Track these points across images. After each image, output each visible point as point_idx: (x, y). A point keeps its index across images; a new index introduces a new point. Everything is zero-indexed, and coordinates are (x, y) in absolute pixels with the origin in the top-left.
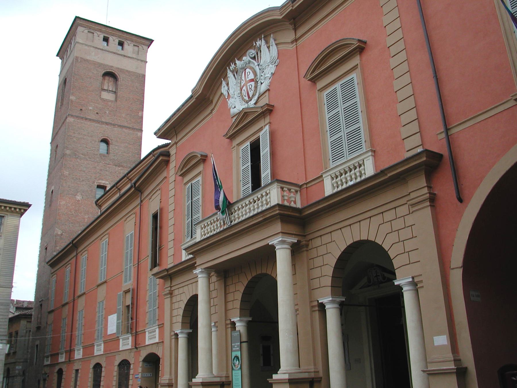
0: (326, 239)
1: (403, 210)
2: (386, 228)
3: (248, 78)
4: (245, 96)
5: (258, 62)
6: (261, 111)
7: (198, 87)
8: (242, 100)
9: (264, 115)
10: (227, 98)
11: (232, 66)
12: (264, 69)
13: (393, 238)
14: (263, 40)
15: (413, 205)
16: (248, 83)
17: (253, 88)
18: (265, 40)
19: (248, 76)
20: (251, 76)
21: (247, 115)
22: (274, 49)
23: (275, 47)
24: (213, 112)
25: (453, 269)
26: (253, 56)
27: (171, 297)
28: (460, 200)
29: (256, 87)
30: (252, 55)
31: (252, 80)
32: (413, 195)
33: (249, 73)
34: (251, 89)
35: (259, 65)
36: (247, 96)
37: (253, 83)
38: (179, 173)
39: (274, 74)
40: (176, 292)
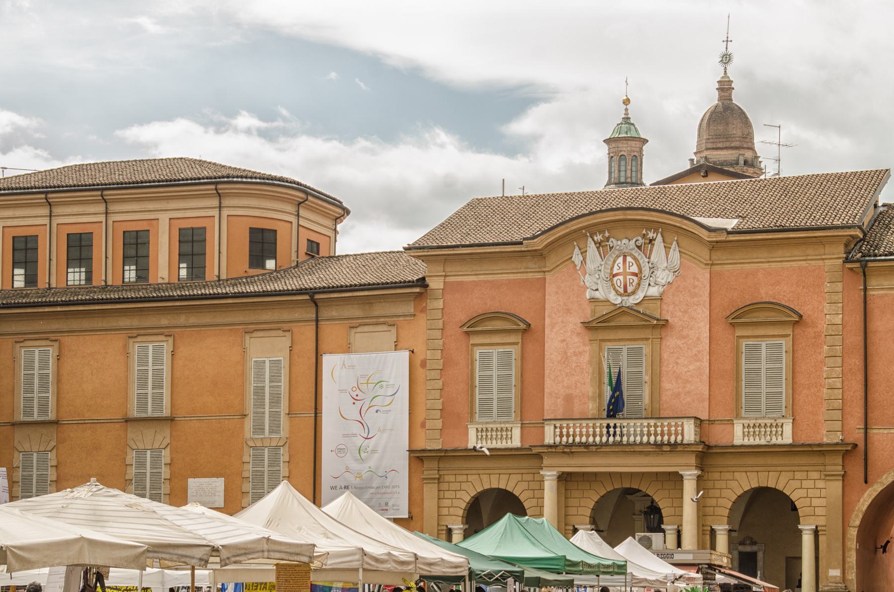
0: (728, 476)
1: (815, 475)
2: (797, 484)
4: (619, 287)
5: (649, 258)
10: (578, 268)
11: (598, 238)
13: (802, 493)
15: (826, 475)
16: (629, 275)
17: (634, 284)
18: (662, 236)
19: (629, 266)
20: (634, 269)
22: (675, 254)
23: (677, 254)
25: (851, 527)
27: (439, 483)
28: (866, 482)
29: (639, 284)
31: (635, 275)
32: (828, 468)
33: (631, 264)
35: (649, 263)
36: (623, 289)
37: (635, 278)
38: (465, 329)
40: (447, 478)
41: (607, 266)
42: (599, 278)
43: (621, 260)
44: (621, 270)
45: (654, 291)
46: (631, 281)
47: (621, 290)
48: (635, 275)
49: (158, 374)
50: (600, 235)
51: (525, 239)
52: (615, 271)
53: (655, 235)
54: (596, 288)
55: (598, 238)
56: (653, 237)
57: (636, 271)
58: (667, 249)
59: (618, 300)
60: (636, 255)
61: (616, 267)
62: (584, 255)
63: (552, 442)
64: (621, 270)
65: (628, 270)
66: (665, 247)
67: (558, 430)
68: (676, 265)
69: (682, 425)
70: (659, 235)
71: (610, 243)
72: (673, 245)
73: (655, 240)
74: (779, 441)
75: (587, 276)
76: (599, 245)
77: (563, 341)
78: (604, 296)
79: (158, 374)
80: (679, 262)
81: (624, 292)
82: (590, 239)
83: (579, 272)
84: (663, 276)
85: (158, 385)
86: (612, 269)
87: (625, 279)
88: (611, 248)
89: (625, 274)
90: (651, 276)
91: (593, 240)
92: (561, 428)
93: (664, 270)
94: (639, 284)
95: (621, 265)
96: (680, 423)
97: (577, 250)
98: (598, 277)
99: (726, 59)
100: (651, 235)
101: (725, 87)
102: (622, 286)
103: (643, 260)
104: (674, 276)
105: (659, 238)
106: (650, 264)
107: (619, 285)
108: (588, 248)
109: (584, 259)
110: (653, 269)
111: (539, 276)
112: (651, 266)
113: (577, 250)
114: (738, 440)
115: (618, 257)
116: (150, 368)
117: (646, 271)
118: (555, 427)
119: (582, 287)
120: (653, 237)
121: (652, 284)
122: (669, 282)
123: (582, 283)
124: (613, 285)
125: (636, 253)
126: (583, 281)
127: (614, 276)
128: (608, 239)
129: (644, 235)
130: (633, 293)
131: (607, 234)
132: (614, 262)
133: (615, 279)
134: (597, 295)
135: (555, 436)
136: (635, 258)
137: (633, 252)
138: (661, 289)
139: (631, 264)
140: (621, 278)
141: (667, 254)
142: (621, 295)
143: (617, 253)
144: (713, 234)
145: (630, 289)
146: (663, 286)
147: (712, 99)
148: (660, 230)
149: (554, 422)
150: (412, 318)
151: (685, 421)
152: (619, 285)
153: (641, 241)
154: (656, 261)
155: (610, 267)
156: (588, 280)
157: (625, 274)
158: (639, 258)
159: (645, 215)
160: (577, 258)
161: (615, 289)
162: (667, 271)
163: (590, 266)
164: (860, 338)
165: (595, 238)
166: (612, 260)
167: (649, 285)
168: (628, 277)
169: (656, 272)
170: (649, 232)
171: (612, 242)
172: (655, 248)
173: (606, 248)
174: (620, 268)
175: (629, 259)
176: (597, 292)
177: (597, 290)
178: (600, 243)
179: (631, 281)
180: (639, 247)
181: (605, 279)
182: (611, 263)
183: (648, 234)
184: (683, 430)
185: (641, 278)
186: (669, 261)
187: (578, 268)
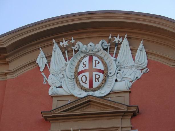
3: (95, 66)
4: (85, 83)
5: (116, 57)
6: (126, 110)
7: (6, 39)
8: (75, 82)
9: (123, 116)
10: (42, 70)
11: (65, 43)
12: (121, 68)
14: (125, 39)
16: (95, 72)
17: (101, 79)
19: (95, 64)
20: (101, 66)
21: (90, 104)
24: (8, 76)
26: (106, 47)
29: (105, 81)
30: (105, 46)
31: (102, 72)
33: (97, 62)
34: (98, 79)
35: (115, 61)
37: (102, 75)
39: (139, 79)
41: (72, 67)
42: (63, 77)
43: (87, 59)
44: (87, 67)
45: (123, 86)
46: (97, 77)
47: (87, 86)
48: (102, 72)
50: (66, 41)
52: (80, 69)
53: (121, 40)
54: (60, 85)
55: (65, 43)
56: (119, 41)
57: (103, 69)
58: (134, 52)
60: (102, 56)
61: (81, 65)
62: (49, 59)
64: (87, 67)
65: (94, 67)
66: (131, 49)
68: (143, 63)
70: (125, 39)
71: (76, 46)
72: (139, 49)
73: (121, 44)
75: (50, 76)
76: (64, 50)
78: (69, 92)
80: (146, 61)
81: (89, 87)
82: (56, 45)
83: (43, 74)
86: (77, 67)
88: (76, 52)
90: (117, 73)
93: (132, 68)
95: (87, 64)
97: (42, 54)
98: (62, 76)
100: (117, 39)
102: (88, 82)
103: (109, 59)
104: (142, 73)
105: (125, 42)
106: (117, 62)
107: (84, 81)
108: (53, 52)
109: (49, 63)
110: (120, 68)
112: (117, 64)
113: (42, 54)
115: (85, 57)
117: (112, 69)
119: (45, 85)
120: (119, 41)
121: (118, 80)
122: (137, 78)
123: (45, 83)
124: (77, 82)
125: (103, 54)
126: (46, 81)
127: (79, 74)
128: (73, 45)
129: (110, 40)
130: (99, 88)
131: (73, 41)
132: (80, 61)
133: (80, 76)
134: (61, 92)
137: (99, 54)
139: (97, 62)
140: (87, 74)
141: (134, 57)
142: (86, 90)
143: (82, 55)
145: (95, 85)
146: (131, 81)
148: (126, 36)
152: (84, 81)
154: (123, 60)
155: (74, 67)
156: (52, 80)
157: (90, 70)
158: (105, 59)
160: (41, 61)
161: (79, 85)
162: (134, 69)
163: (53, 68)
165: (61, 44)
166: (77, 61)
167: (116, 80)
168: (94, 73)
169: (122, 70)
170: (115, 37)
171: (78, 45)
172: (120, 51)
173: (71, 54)
174: (85, 66)
175: (94, 58)
176: (61, 89)
177: (61, 87)
179: (97, 77)
180: (106, 50)
181: (70, 77)
182: (75, 64)
183: (114, 39)
185: (108, 76)
187: (42, 70)
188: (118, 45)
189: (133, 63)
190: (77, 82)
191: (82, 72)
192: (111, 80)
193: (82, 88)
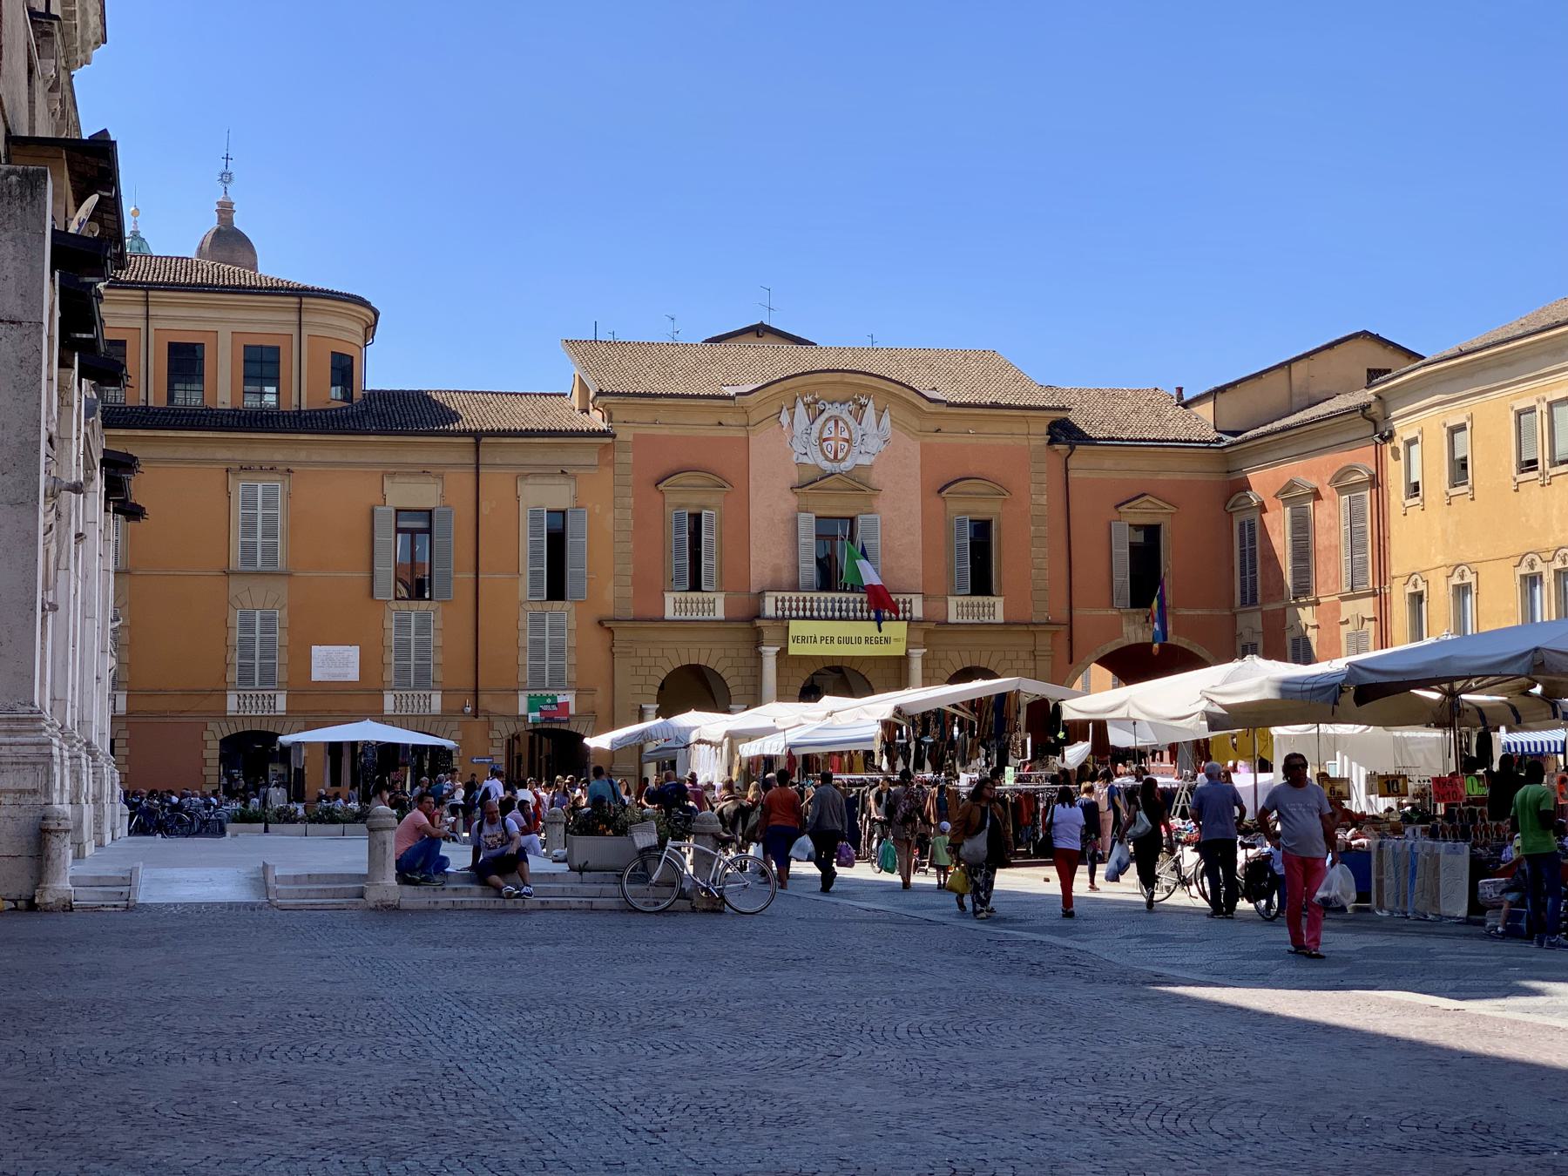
5: (860, 424)
14: (871, 402)
20: (846, 435)
22: (886, 420)
28: (1071, 662)
29: (848, 451)
31: (847, 441)
37: (846, 444)
43: (832, 423)
47: (831, 456)
48: (847, 441)
49: (270, 520)
51: (737, 394)
55: (809, 399)
59: (827, 466)
60: (847, 420)
63: (774, 615)
67: (780, 604)
69: (910, 602)
74: (992, 620)
77: (770, 506)
79: (270, 520)
84: (874, 444)
85: (270, 532)
86: (821, 433)
87: (836, 444)
89: (836, 439)
91: (803, 400)
92: (783, 600)
94: (848, 451)
95: (833, 430)
96: (908, 600)
99: (226, 177)
100: (863, 400)
101: (225, 210)
111: (742, 434)
114: (952, 618)
116: (260, 511)
117: (857, 436)
118: (777, 601)
124: (822, 450)
127: (825, 440)
130: (843, 459)
133: (825, 444)
135: (777, 609)
136: (846, 423)
138: (873, 458)
140: (832, 443)
142: (831, 461)
144: (933, 405)
147: (213, 223)
149: (775, 594)
150: (596, 472)
151: (913, 596)
153: (853, 407)
159: (864, 380)
161: (824, 454)
164: (1063, 520)
175: (840, 423)
177: (806, 454)
178: (809, 405)
184: (911, 607)
186: (881, 428)
188: (863, 406)
189: (875, 431)
190: (822, 450)
191: (825, 440)
192: (855, 451)
193: (827, 458)
